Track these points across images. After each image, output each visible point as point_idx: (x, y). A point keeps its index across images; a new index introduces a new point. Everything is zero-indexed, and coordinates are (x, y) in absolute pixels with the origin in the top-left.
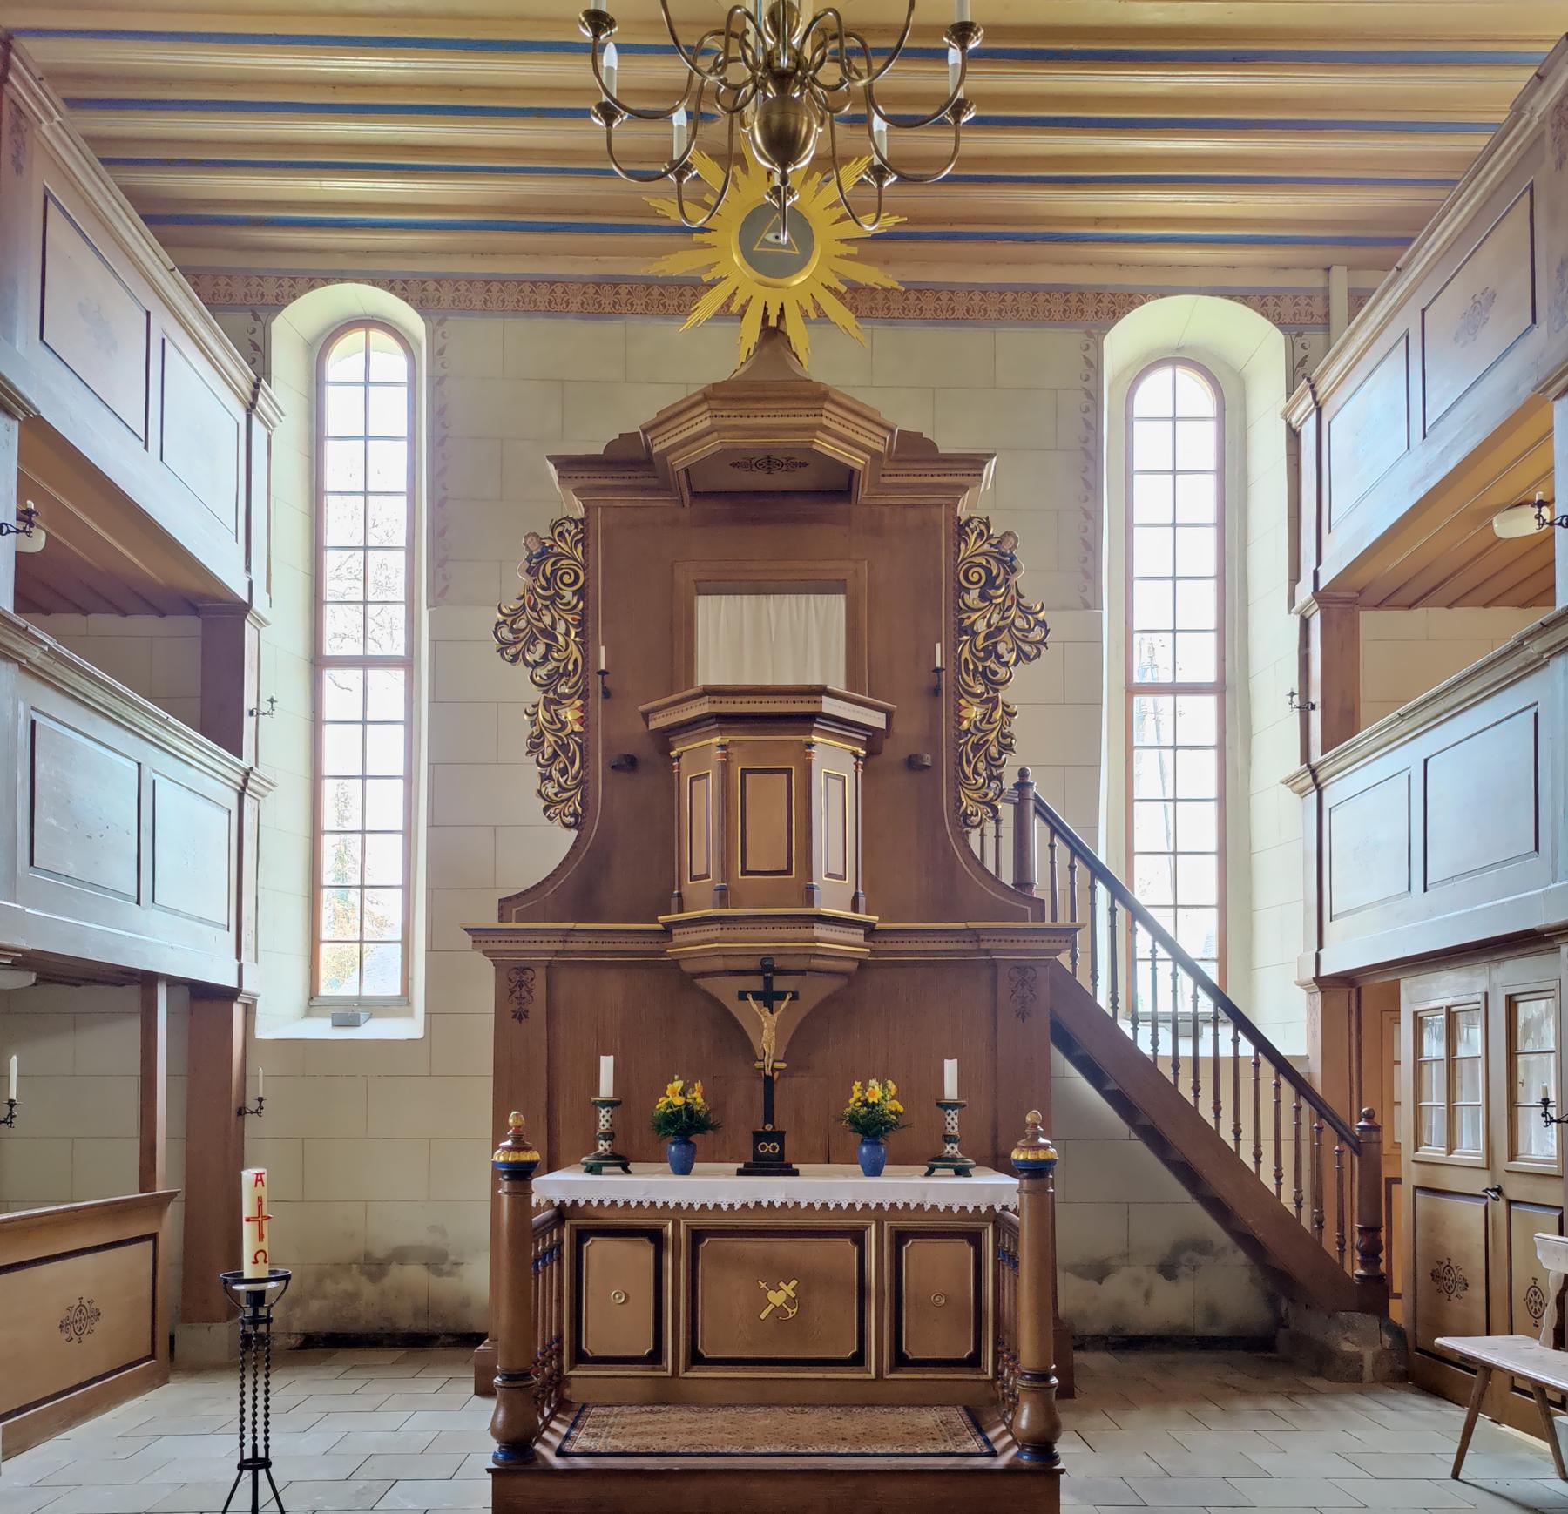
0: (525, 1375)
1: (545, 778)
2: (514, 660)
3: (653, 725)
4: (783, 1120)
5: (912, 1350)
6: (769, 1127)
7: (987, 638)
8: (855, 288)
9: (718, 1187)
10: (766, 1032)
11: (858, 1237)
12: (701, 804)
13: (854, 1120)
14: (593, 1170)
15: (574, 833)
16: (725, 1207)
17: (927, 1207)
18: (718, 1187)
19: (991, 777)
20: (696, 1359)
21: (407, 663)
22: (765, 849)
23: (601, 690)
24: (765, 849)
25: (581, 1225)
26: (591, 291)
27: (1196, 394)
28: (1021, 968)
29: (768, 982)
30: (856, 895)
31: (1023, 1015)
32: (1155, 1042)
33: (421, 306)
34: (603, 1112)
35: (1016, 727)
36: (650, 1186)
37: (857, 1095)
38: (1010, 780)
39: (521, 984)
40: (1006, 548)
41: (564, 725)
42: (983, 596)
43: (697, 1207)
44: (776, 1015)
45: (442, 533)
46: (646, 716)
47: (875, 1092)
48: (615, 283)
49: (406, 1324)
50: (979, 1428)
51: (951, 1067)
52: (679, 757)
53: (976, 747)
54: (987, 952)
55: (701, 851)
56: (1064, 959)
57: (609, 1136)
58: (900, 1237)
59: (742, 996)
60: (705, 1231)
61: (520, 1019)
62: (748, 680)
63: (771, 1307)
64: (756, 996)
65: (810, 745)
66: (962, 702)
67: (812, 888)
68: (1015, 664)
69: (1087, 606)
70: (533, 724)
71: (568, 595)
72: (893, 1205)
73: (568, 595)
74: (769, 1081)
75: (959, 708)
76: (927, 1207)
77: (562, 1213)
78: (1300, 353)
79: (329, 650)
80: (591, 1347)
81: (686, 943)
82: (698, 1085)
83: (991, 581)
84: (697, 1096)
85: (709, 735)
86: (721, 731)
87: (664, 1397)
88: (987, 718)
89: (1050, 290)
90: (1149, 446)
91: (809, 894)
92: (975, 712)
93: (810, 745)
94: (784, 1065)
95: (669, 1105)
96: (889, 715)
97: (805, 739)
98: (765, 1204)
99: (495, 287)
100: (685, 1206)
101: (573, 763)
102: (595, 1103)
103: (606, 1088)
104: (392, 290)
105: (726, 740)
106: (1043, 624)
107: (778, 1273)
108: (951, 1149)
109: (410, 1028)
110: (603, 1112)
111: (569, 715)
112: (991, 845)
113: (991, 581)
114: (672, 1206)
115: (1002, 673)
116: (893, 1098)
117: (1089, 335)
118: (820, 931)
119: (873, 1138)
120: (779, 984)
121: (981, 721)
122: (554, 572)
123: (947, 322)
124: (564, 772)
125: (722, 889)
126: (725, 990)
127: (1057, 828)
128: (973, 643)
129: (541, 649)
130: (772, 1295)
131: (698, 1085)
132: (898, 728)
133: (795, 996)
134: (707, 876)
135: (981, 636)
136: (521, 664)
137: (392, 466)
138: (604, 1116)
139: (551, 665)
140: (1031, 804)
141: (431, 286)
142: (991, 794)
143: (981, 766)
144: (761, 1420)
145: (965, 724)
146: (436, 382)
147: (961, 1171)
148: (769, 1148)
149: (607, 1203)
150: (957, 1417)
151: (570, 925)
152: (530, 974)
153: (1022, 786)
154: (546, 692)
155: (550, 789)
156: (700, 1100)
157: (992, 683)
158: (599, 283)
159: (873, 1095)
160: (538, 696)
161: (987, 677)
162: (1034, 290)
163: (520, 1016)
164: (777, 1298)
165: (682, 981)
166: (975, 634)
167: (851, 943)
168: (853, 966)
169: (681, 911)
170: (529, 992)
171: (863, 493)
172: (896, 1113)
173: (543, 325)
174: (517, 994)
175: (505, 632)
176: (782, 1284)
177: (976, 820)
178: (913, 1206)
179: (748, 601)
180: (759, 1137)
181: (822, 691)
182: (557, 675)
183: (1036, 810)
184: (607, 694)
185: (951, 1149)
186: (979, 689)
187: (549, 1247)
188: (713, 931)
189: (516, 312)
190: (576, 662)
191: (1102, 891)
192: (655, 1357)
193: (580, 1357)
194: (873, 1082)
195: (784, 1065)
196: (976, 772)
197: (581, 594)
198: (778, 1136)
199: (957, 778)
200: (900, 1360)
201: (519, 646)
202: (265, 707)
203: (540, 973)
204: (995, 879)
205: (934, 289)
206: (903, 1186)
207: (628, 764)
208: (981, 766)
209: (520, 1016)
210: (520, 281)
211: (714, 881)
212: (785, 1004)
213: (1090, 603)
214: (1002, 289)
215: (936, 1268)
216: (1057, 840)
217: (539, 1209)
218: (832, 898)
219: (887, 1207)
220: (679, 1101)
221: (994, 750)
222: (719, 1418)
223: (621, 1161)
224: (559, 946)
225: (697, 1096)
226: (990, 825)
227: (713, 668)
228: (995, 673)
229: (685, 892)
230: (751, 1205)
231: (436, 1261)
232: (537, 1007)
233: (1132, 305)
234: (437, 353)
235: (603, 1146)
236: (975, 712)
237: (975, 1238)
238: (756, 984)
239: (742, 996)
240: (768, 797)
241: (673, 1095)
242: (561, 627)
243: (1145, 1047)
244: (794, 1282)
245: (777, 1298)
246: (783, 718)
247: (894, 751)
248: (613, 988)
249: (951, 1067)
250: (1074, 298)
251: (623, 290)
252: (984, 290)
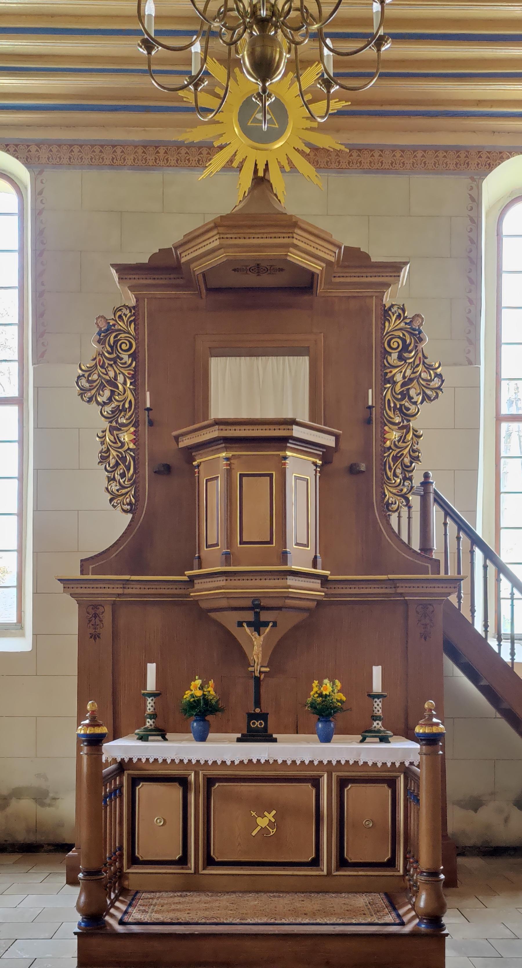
0: (98, 872)
1: (110, 479)
2: (90, 400)
3: (182, 445)
4: (266, 706)
5: (350, 856)
6: (258, 710)
7: (403, 385)
8: (315, 149)
9: (225, 749)
10: (256, 648)
11: (316, 782)
12: (213, 496)
13: (313, 706)
14: (142, 738)
15: (130, 516)
16: (228, 763)
17: (361, 763)
18: (225, 749)
19: (405, 479)
20: (210, 861)
21: (19, 401)
22: (256, 526)
23: (148, 421)
24: (256, 526)
25: (134, 774)
26: (140, 151)
28: (425, 605)
29: (257, 615)
30: (316, 557)
31: (425, 636)
32: (513, 654)
33: (27, 162)
34: (149, 700)
35: (422, 445)
36: (180, 749)
37: (315, 689)
38: (417, 480)
39: (96, 616)
40: (415, 325)
41: (123, 444)
42: (400, 358)
43: (210, 763)
44: (262, 636)
45: (42, 315)
46: (177, 439)
47: (327, 687)
48: (156, 145)
49: (21, 837)
50: (394, 906)
51: (377, 671)
52: (198, 466)
53: (395, 459)
54: (401, 594)
55: (213, 529)
56: (453, 599)
57: (153, 716)
58: (343, 783)
59: (240, 624)
60: (214, 779)
61: (95, 639)
62: (244, 415)
63: (259, 828)
64: (249, 624)
65: (285, 458)
66: (386, 428)
67: (285, 554)
68: (422, 403)
69: (470, 363)
70: (102, 443)
71: (125, 357)
72: (339, 762)
73: (125, 357)
74: (257, 680)
75: (384, 432)
76: (361, 763)
77: (122, 766)
80: (140, 854)
81: (203, 590)
82: (211, 682)
83: (405, 348)
84: (211, 690)
85: (218, 451)
86: (226, 449)
87: (190, 886)
88: (402, 439)
89: (447, 149)
91: (284, 557)
92: (394, 435)
93: (285, 458)
94: (267, 669)
95: (192, 696)
96: (337, 437)
97: (281, 454)
98: (255, 761)
99: (76, 149)
100: (202, 762)
101: (129, 470)
102: (144, 694)
103: (151, 685)
104: (7, 151)
105: (230, 454)
106: (440, 376)
107: (262, 806)
108: (377, 725)
109: (22, 644)
110: (149, 700)
111: (126, 437)
112: (405, 524)
113: (405, 348)
114: (194, 762)
115: (413, 409)
116: (339, 691)
117: (472, 179)
118: (291, 581)
119: (326, 717)
120: (265, 616)
121: (399, 441)
122: (116, 342)
123: (378, 171)
124: (123, 475)
125: (227, 555)
126: (229, 620)
127: (448, 512)
128: (393, 389)
129: (107, 393)
130: (259, 820)
131: (211, 682)
132: (342, 445)
133: (275, 624)
134: (217, 545)
135: (399, 385)
136: (94, 404)
138: (150, 703)
139: (114, 404)
140: (432, 496)
141: (33, 148)
142: (405, 490)
143: (398, 471)
144: (252, 901)
145: (388, 443)
146: (37, 213)
147: (384, 739)
148: (258, 724)
149: (151, 760)
150: (380, 900)
151: (127, 577)
152: (101, 609)
153: (426, 484)
154: (111, 422)
155: (114, 487)
156: (212, 692)
157: (406, 415)
158: (145, 146)
159: (326, 689)
160: (106, 425)
161: (403, 412)
162: (436, 149)
163: (95, 636)
164: (262, 822)
165: (200, 614)
166: (395, 383)
167: (312, 589)
168: (313, 604)
169: (200, 567)
170: (101, 621)
171: (321, 288)
172: (341, 701)
173: (108, 174)
174: (93, 622)
175: (84, 382)
176: (266, 813)
177: (395, 507)
178: (351, 762)
179: (244, 361)
180: (252, 717)
181: (293, 422)
182: (117, 411)
183: (435, 500)
184: (151, 423)
185: (377, 725)
186: (397, 420)
187: (114, 788)
188: (221, 581)
189: (91, 166)
190: (130, 402)
191: (479, 554)
192: (183, 861)
193: (134, 861)
194: (326, 681)
195: (267, 669)
196: (395, 475)
197: (134, 356)
198: (264, 717)
199: (383, 479)
200: (343, 863)
201: (93, 392)
204: (408, 547)
205: (370, 149)
206: (346, 749)
207: (166, 470)
208: (398, 471)
209: (95, 636)
210: (93, 145)
211: (222, 548)
212: (268, 629)
213: (472, 360)
214: (414, 149)
215: (366, 801)
216: (449, 521)
217: (107, 764)
218: (300, 558)
219: (334, 763)
220: (199, 693)
221: (407, 461)
222: (225, 900)
223: (161, 733)
224: (120, 591)
225: (211, 690)
226: (404, 511)
227: (221, 406)
228: (408, 409)
229: (203, 555)
230: (246, 762)
231: (41, 797)
234: (38, 193)
235: (149, 723)
236: (394, 435)
237: (392, 783)
238: (249, 616)
239: (240, 624)
240: (257, 492)
241: (195, 690)
242: (120, 379)
243: (506, 657)
244: (274, 812)
245: (262, 822)
246: (266, 441)
247: (340, 462)
248: (155, 619)
249: (377, 671)
250: (463, 155)
251: (162, 150)
252: (403, 149)
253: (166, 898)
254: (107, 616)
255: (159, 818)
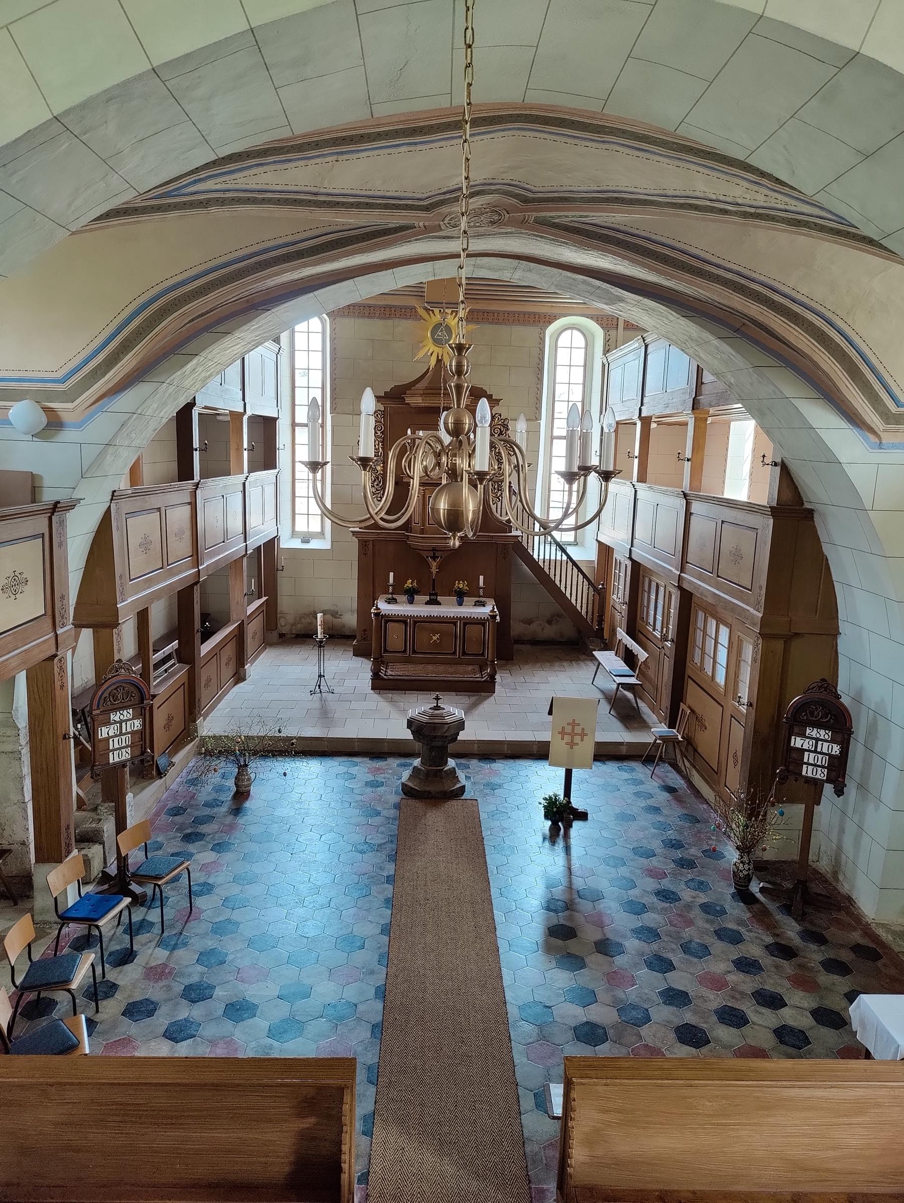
20: (414, 652)
27: (579, 339)
28: (505, 545)
47: (461, 586)
48: (391, 307)
51: (481, 577)
58: (465, 624)
60: (417, 622)
78: (608, 338)
79: (297, 421)
87: (407, 661)
90: (562, 356)
113: (501, 433)
119: (461, 596)
123: (496, 323)
126: (424, 554)
137: (316, 361)
144: (430, 667)
146: (333, 340)
150: (477, 667)
158: (385, 307)
164: (435, 638)
173: (367, 321)
193: (386, 651)
200: (464, 654)
202: (281, 447)
203: (371, 543)
222: (420, 667)
232: (370, 552)
233: (556, 319)
234: (333, 330)
241: (408, 584)
245: (435, 638)
253: (398, 666)
254: (371, 547)
255: (395, 636)
